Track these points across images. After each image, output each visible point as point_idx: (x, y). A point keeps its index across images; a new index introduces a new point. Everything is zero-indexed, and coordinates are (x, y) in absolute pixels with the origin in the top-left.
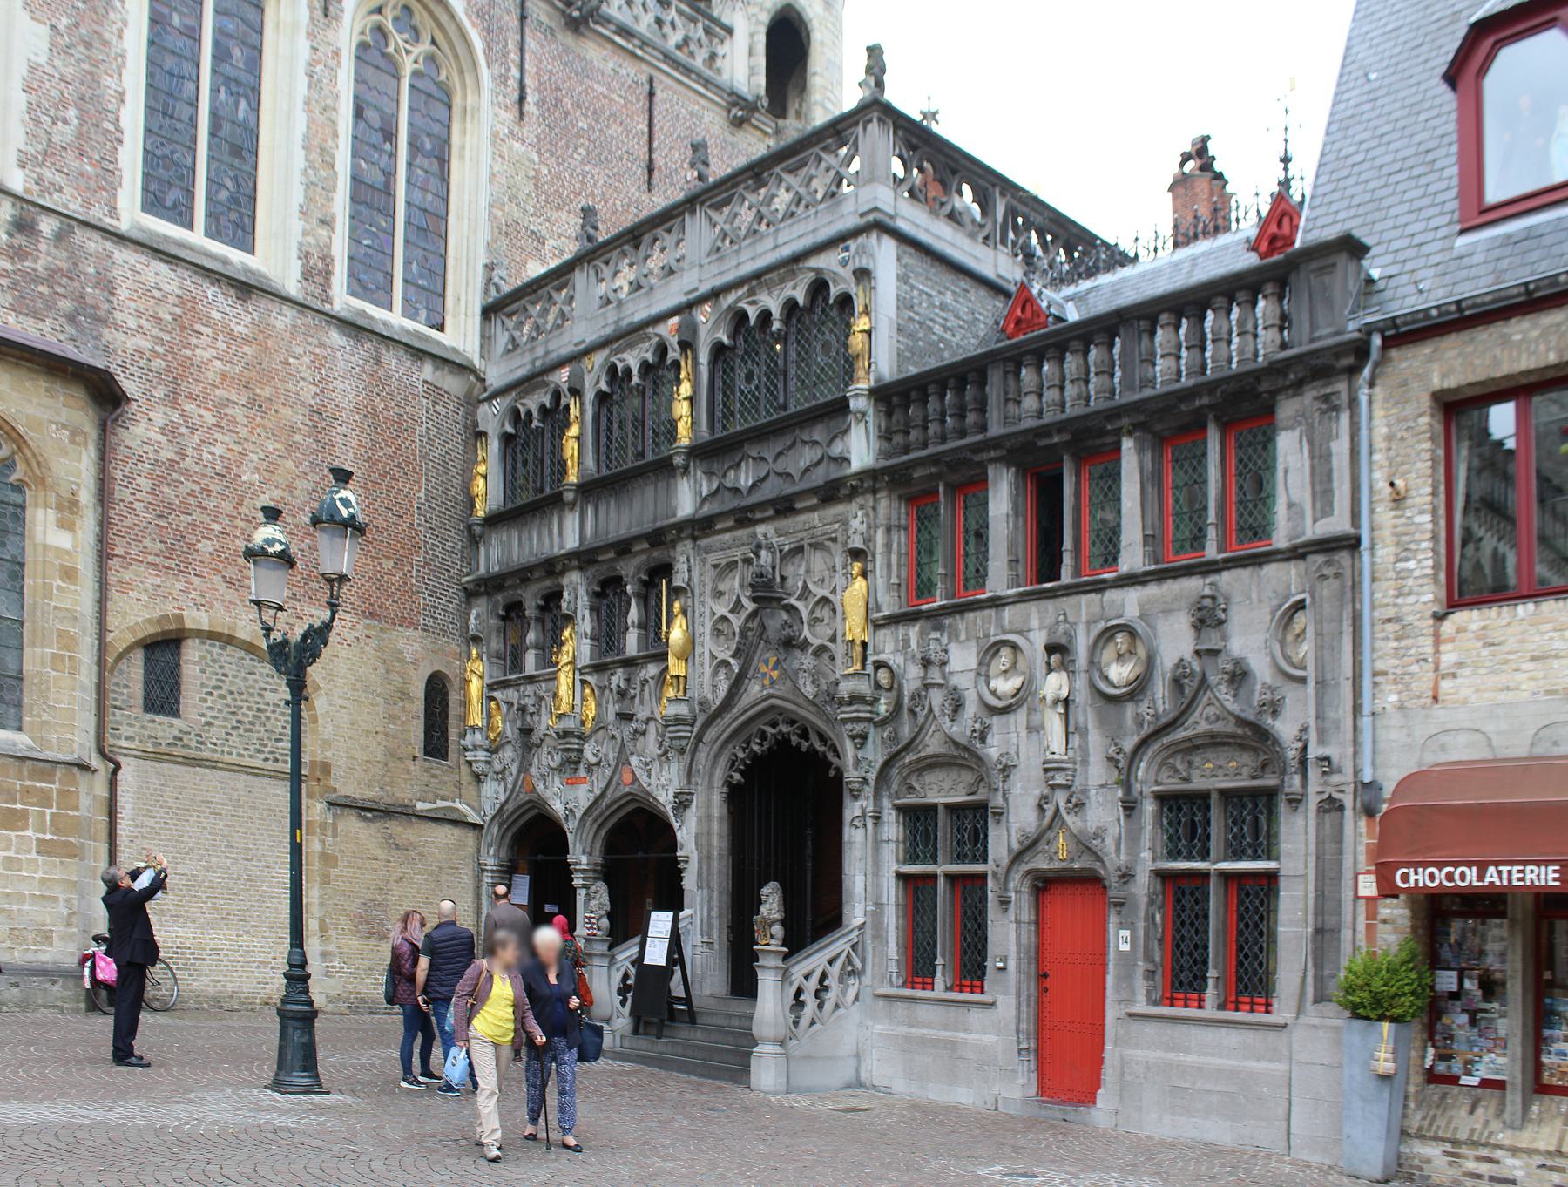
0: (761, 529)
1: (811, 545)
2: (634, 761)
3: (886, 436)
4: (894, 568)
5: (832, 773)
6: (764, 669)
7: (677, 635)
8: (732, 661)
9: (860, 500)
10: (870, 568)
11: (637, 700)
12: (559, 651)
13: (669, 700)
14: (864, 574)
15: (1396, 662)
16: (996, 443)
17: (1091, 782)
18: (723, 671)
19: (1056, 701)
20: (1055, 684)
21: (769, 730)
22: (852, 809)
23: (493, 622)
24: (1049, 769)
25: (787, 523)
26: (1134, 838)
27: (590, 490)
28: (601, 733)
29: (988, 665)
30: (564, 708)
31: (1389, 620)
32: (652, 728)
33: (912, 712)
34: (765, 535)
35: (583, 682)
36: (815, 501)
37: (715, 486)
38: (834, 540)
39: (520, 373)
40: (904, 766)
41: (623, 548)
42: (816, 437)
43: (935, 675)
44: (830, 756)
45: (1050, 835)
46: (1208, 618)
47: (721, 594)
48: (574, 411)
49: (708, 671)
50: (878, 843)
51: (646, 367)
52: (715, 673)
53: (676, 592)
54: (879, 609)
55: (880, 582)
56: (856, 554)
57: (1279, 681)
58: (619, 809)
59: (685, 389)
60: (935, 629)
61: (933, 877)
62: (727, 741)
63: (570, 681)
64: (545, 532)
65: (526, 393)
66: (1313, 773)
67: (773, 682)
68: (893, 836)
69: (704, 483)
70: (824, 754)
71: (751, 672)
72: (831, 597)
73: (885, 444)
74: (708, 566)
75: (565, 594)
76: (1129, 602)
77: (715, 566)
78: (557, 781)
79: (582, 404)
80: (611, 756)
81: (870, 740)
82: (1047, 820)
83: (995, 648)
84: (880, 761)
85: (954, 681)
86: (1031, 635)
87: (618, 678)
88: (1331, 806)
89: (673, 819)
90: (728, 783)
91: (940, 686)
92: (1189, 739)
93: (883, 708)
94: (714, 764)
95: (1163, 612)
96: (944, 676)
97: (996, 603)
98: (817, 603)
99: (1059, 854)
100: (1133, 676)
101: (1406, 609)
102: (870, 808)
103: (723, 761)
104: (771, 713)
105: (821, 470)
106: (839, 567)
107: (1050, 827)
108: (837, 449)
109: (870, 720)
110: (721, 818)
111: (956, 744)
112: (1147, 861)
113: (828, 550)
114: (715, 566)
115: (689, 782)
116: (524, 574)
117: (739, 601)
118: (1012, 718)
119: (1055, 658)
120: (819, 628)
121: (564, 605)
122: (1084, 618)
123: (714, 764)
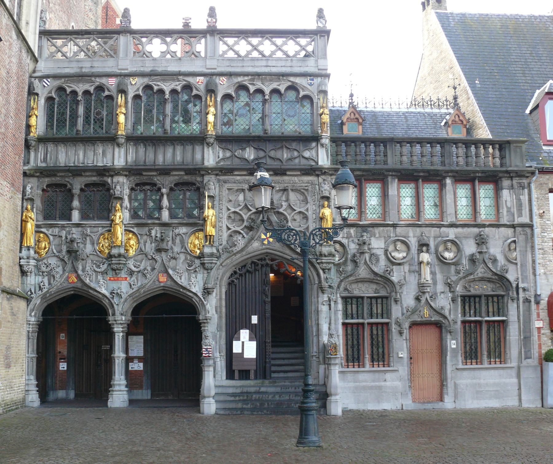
6: (263, 236)
8: (242, 232)
9: (323, 177)
15: (542, 261)
17: (438, 291)
20: (425, 257)
23: (40, 192)
28: (140, 256)
31: (540, 249)
33: (355, 262)
36: (299, 173)
37: (228, 154)
38: (307, 190)
39: (67, 71)
41: (165, 172)
46: (481, 241)
47: (230, 201)
48: (120, 100)
50: (336, 311)
57: (507, 263)
59: (212, 110)
60: (364, 232)
61: (363, 324)
66: (521, 291)
71: (256, 238)
72: (306, 212)
75: (118, 187)
76: (452, 233)
77: (228, 189)
79: (126, 99)
84: (339, 280)
85: (374, 251)
86: (410, 239)
88: (527, 301)
93: (337, 259)
95: (464, 237)
99: (426, 313)
101: (545, 246)
103: (228, 274)
105: (297, 161)
108: (307, 154)
111: (375, 274)
112: (460, 318)
114: (228, 189)
118: (402, 267)
119: (424, 249)
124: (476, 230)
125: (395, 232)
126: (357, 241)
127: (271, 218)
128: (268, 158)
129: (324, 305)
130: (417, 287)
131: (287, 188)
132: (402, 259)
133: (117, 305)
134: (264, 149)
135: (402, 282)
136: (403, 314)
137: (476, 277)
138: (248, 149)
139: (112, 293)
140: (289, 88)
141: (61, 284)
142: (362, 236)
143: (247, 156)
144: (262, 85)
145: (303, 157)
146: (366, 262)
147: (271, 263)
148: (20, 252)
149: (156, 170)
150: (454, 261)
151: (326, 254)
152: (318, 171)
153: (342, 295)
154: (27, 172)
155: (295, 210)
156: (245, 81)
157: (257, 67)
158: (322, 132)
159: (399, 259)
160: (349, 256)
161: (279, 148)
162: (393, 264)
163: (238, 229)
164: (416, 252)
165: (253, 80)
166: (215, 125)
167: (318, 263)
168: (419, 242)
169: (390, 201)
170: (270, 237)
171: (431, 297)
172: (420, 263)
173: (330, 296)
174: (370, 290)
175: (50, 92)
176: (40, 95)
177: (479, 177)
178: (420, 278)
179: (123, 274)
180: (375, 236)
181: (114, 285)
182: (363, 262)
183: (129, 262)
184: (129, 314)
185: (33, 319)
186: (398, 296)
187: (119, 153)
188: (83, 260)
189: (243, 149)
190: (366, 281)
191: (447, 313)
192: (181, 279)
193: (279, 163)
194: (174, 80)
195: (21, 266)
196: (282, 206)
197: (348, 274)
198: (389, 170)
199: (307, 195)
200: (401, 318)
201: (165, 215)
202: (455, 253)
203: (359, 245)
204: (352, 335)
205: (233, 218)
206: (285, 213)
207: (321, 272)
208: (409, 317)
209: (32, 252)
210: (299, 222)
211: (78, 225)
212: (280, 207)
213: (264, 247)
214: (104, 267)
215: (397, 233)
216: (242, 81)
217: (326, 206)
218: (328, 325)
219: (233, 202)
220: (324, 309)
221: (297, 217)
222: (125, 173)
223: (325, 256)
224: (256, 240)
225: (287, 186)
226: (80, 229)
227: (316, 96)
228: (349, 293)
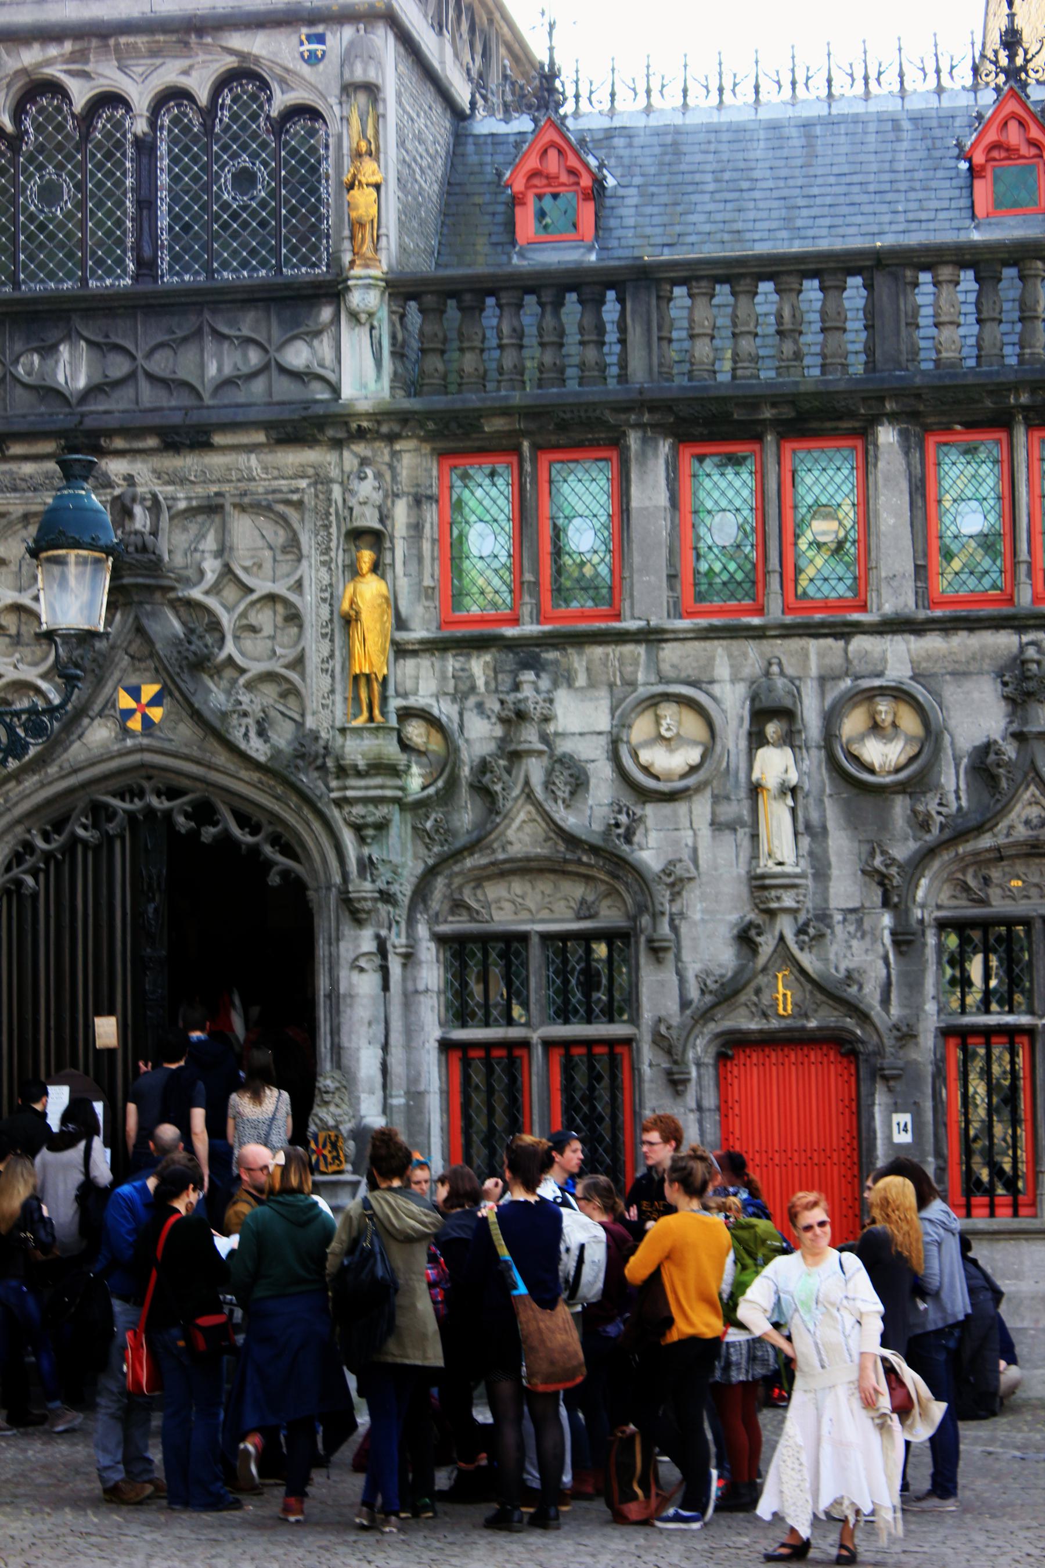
4: (427, 561)
5: (274, 879)
6: (125, 701)
8: (44, 685)
9: (361, 448)
10: (388, 560)
14: (376, 568)
17: (833, 904)
25: (188, 463)
26: (913, 984)
33: (483, 791)
34: (130, 479)
36: (260, 437)
38: (299, 505)
42: (246, 332)
43: (529, 736)
45: (762, 980)
55: (403, 584)
60: (525, 666)
62: (19, 821)
70: (255, 850)
71: (97, 707)
72: (293, 597)
81: (394, 830)
84: (420, 869)
85: (564, 747)
91: (540, 753)
92: (998, 849)
93: (415, 782)
95: (953, 674)
96: (544, 738)
100: (903, 759)
105: (258, 386)
108: (298, 356)
111: (571, 840)
113: (284, 521)
118: (682, 807)
119: (772, 729)
120: (248, 643)
122: (814, 671)
124: (1005, 641)
125: (654, 663)
126: (497, 707)
127: (154, 628)
128: (144, 385)
129: (362, 970)
130: (744, 891)
131: (220, 500)
132: (683, 776)
134: (131, 347)
135: (679, 871)
136: (685, 1004)
137: (1002, 840)
138: (64, 349)
140: (224, 82)
142: (516, 687)
143: (61, 379)
144: (119, 76)
145: (283, 370)
146: (529, 796)
147: (167, 804)
150: (902, 776)
151: (361, 764)
152: (333, 424)
155: (251, 591)
156: (49, 62)
158: (352, 263)
160: (466, 771)
161: (185, 340)
162: (645, 795)
164: (743, 744)
167: (339, 803)
168: (753, 700)
169: (635, 535)
170: (156, 701)
171: (801, 931)
172: (755, 790)
173: (383, 933)
174: (561, 908)
177: (1025, 408)
178: (755, 856)
180: (570, 685)
182: (516, 792)
186: (665, 929)
189: (48, 351)
190: (541, 871)
191: (871, 995)
193: (185, 399)
196: (202, 573)
198: (627, 408)
199: (296, 525)
200: (675, 1021)
202: (909, 739)
203: (504, 721)
204: (490, 1091)
205: (13, 631)
206: (212, 602)
207: (348, 837)
208: (706, 1015)
210: (272, 638)
212: (194, 577)
213: (129, 742)
215: (666, 668)
216: (40, 65)
218: (380, 1052)
221: (265, 618)
223: (359, 774)
224: (100, 714)
225: (218, 494)
227: (336, 109)
228: (473, 920)
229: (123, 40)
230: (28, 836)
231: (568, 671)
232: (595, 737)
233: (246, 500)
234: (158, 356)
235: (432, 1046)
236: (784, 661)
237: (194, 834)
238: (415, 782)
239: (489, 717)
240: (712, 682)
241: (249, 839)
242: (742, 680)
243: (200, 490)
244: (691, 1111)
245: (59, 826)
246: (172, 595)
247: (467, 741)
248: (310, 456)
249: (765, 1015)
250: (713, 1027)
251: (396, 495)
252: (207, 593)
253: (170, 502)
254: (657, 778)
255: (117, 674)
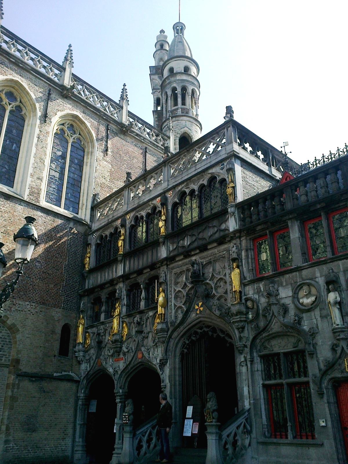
0: (193, 258)
1: (214, 261)
2: (143, 349)
3: (242, 220)
6: (197, 307)
7: (161, 299)
8: (183, 306)
9: (234, 242)
10: (240, 264)
11: (144, 326)
12: (114, 311)
13: (158, 323)
14: (238, 267)
16: (291, 212)
18: (180, 312)
19: (336, 303)
20: (332, 297)
21: (199, 331)
22: (240, 359)
24: (334, 331)
25: (205, 254)
27: (127, 255)
29: (298, 294)
30: (116, 331)
32: (150, 335)
35: (123, 322)
36: (215, 244)
40: (262, 338)
41: (140, 272)
42: (214, 225)
44: (226, 338)
45: (340, 361)
47: (178, 283)
49: (173, 311)
51: (148, 215)
52: (176, 312)
53: (160, 284)
54: (245, 278)
56: (234, 260)
58: (129, 375)
60: (272, 283)
61: (281, 385)
62: (182, 337)
63: (118, 321)
64: (110, 272)
65: (105, 230)
67: (200, 311)
68: (260, 368)
69: (171, 247)
71: (192, 309)
72: (224, 278)
73: (242, 223)
74: (173, 274)
75: (118, 291)
77: (175, 274)
78: (111, 360)
80: (133, 348)
81: (246, 329)
82: (338, 354)
83: (301, 287)
84: (251, 338)
85: (283, 301)
87: (137, 318)
89: (159, 370)
90: (182, 354)
93: (250, 316)
94: (176, 347)
97: (299, 269)
98: (218, 281)
102: (248, 357)
103: (180, 345)
104: (200, 324)
106: (227, 266)
107: (340, 357)
108: (223, 227)
109: (245, 321)
110: (179, 368)
111: (286, 326)
115: (166, 354)
116: (102, 287)
117: (185, 284)
118: (312, 313)
121: (117, 295)
122: (342, 270)
123: (176, 347)
129: (242, 366)
132: (312, 304)
133: (116, 380)
136: (320, 370)
139: (114, 371)
141: (95, 368)
148: (75, 347)
149: (134, 272)
153: (260, 354)
154: (80, 293)
156: (183, 188)
157: (190, 173)
159: (308, 305)
163: (181, 305)
164: (326, 293)
165: (187, 185)
166: (166, 228)
170: (201, 306)
175: (97, 241)
176: (92, 244)
179: (121, 356)
181: (116, 364)
183: (123, 345)
184: (126, 388)
185: (82, 395)
187: (121, 266)
188: (104, 348)
189: (183, 239)
192: (149, 354)
194: (147, 207)
195: (77, 357)
197: (261, 330)
201: (142, 304)
205: (180, 297)
206: (210, 282)
209: (81, 346)
210: (223, 288)
211: (103, 323)
214: (112, 351)
215: (304, 276)
216: (182, 189)
217: (235, 267)
219: (180, 283)
220: (244, 369)
222: (121, 280)
224: (192, 311)
225: (210, 259)
226: (104, 326)
229: (193, 179)
230: (185, 340)
231: (281, 282)
232: (289, 298)
233: (215, 259)
234: (200, 235)
235: (261, 385)
236: (333, 268)
237: (212, 335)
238: (250, 316)
239: (265, 297)
240: (316, 278)
241: (223, 336)
242: (324, 276)
243: (207, 259)
244: (326, 403)
245: (190, 337)
246: (203, 282)
247: (260, 304)
248: (226, 246)
249: (342, 372)
250: (329, 377)
251: (242, 250)
252: (210, 280)
253: (203, 263)
254: (305, 306)
255: (194, 302)
